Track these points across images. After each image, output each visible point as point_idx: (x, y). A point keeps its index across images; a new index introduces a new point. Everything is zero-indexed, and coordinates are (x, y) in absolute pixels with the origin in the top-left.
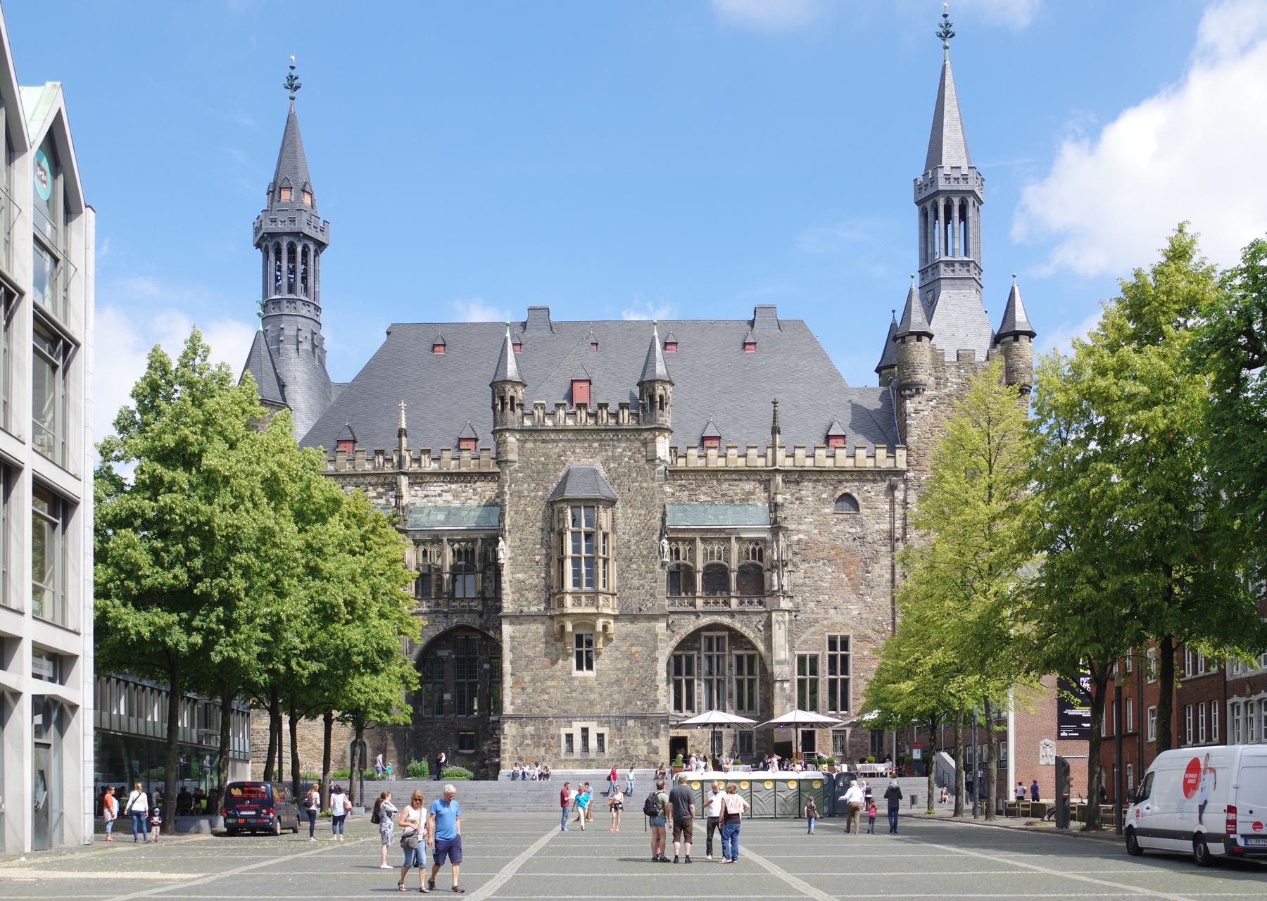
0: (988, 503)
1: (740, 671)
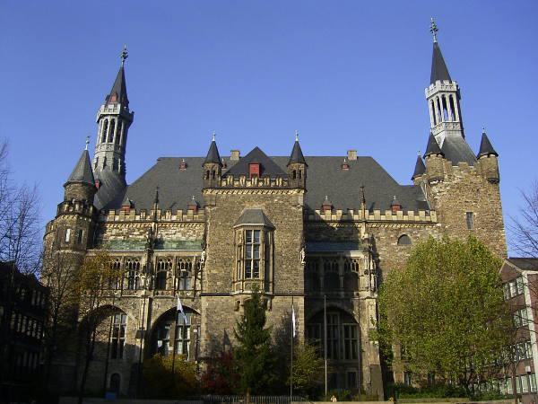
1: (347, 336)
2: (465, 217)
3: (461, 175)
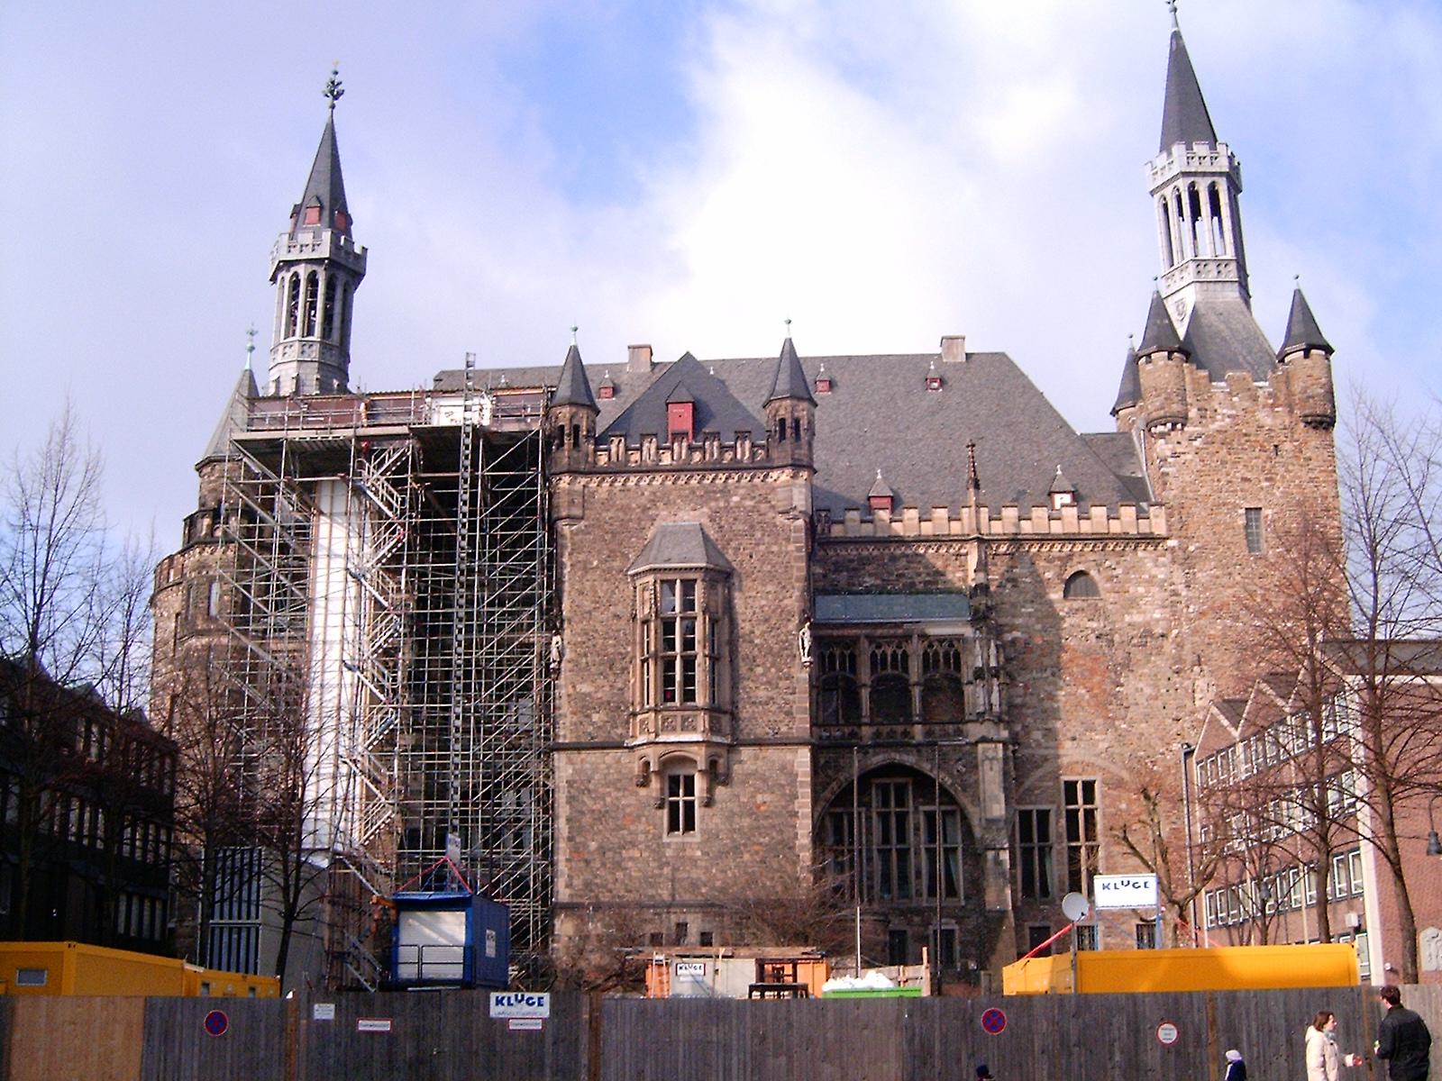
1: (932, 839)
2: (1242, 521)
3: (1233, 407)
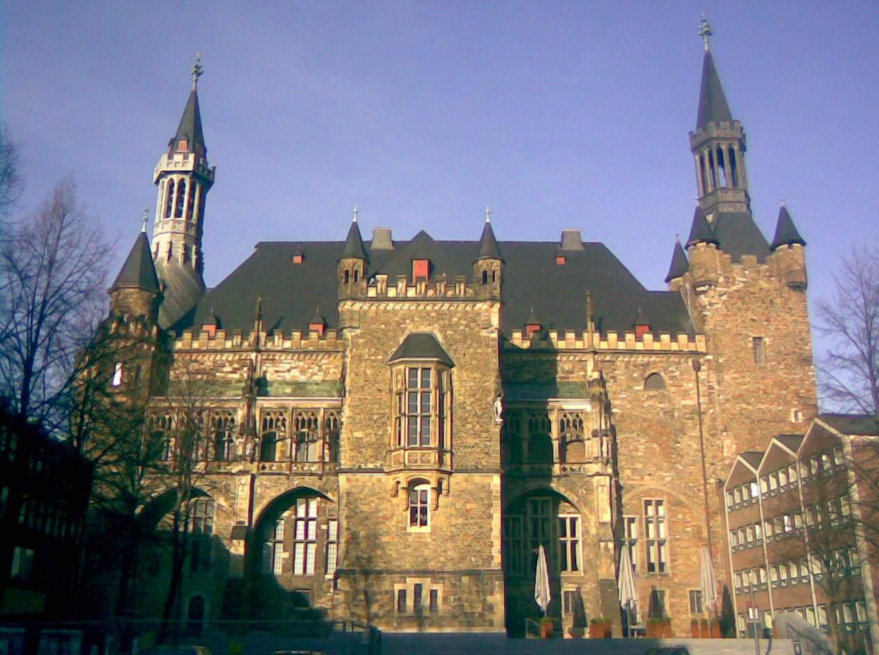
0: (775, 384)
2: (751, 345)
3: (745, 276)
